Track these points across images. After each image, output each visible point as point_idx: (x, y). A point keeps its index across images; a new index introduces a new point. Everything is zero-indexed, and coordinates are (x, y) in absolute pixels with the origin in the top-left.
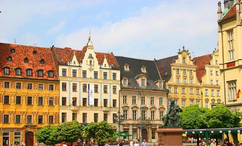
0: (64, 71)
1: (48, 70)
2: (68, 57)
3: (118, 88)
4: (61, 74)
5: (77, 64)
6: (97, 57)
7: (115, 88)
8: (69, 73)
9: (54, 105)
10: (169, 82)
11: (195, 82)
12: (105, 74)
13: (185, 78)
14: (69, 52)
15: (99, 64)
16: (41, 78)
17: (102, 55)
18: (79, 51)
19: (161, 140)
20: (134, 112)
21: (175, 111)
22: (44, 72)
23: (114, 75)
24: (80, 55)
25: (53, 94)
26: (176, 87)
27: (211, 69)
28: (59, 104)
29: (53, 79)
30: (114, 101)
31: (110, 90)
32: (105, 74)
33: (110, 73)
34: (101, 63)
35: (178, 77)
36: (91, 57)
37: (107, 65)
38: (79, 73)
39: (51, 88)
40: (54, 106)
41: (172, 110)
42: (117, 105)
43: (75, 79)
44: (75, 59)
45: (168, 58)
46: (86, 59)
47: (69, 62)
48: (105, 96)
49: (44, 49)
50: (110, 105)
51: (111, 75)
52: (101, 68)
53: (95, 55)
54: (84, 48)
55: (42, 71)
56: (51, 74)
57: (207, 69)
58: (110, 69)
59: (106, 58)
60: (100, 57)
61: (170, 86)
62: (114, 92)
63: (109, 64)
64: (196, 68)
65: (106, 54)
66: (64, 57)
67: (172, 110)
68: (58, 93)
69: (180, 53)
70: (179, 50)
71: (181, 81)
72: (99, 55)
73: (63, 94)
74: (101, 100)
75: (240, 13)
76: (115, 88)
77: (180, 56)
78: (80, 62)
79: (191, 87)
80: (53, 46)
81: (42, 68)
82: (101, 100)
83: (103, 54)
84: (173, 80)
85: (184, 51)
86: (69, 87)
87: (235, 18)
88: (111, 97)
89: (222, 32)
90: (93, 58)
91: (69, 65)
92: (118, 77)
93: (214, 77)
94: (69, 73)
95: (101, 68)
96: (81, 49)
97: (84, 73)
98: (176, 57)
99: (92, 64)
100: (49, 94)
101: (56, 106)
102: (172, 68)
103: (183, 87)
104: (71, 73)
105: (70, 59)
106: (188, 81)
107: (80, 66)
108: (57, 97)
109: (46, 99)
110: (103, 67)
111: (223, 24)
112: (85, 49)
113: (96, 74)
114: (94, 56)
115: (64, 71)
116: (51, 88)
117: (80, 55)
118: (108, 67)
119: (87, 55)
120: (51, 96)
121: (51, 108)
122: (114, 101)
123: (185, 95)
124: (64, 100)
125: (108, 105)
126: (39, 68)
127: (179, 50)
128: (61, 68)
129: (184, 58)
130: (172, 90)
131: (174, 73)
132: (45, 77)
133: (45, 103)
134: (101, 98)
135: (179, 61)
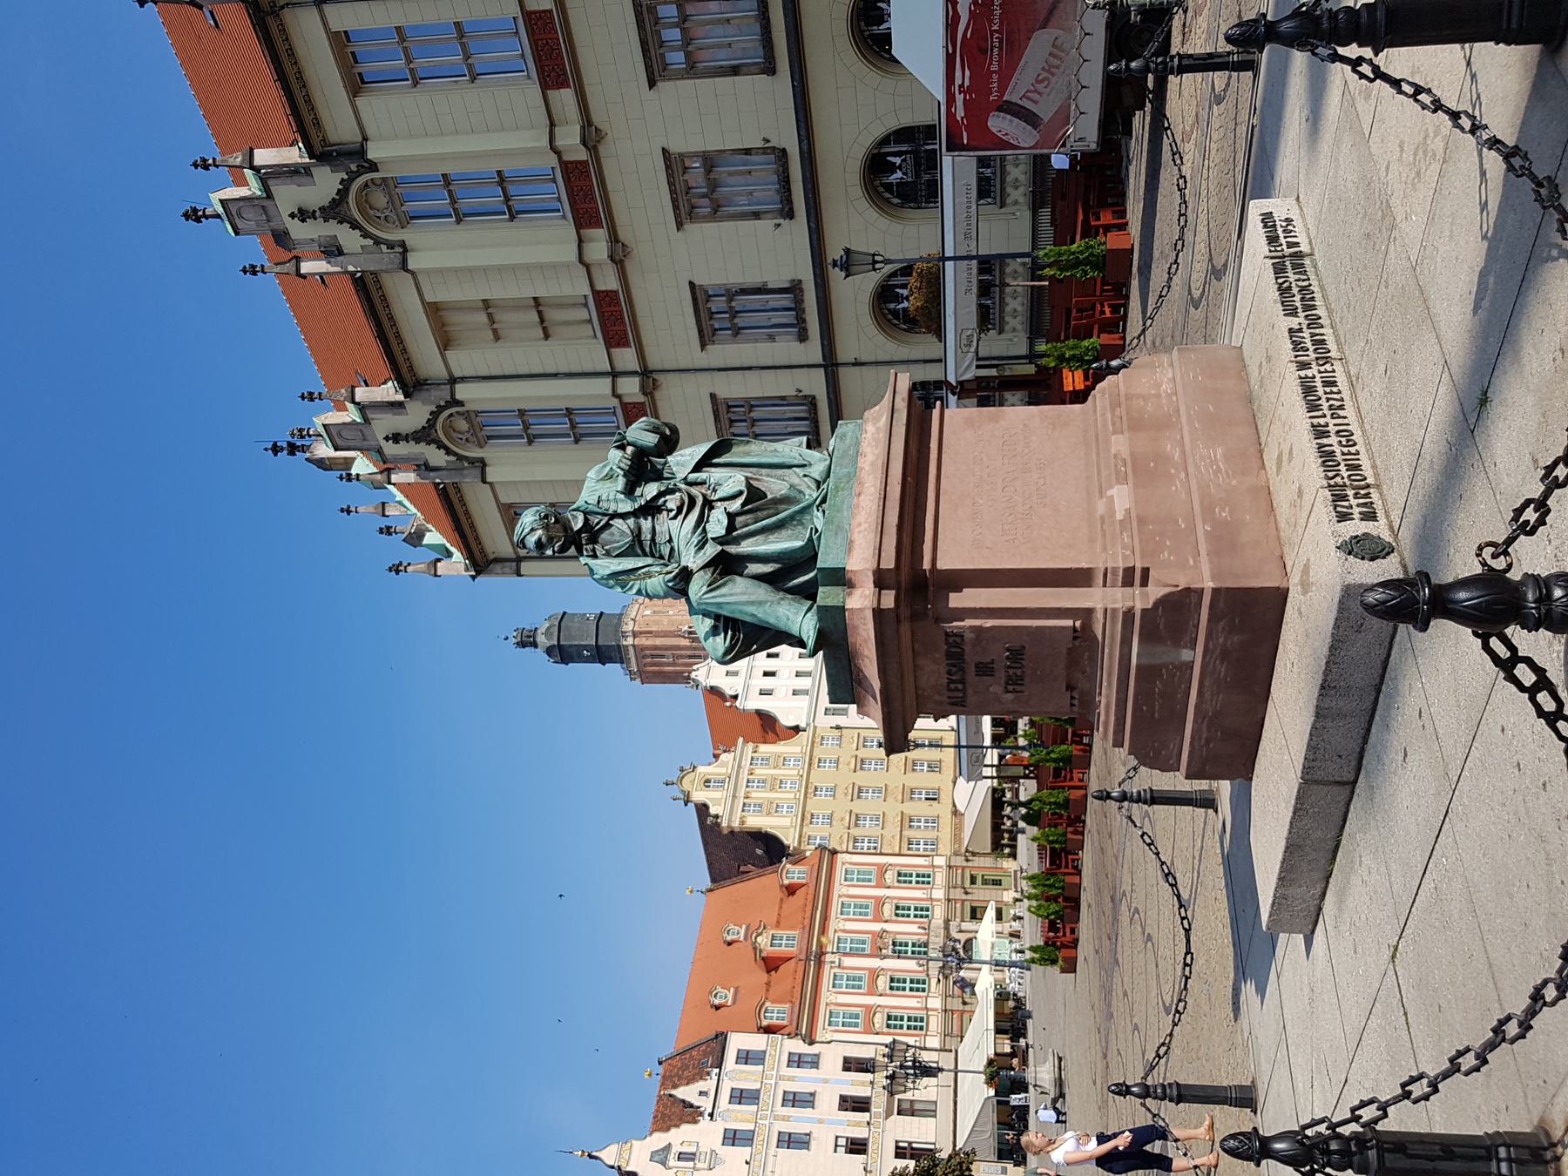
3: (798, 1046)
6: (668, 1129)
7: (797, 1061)
10: (790, 840)
11: (798, 749)
12: (740, 1097)
15: (695, 1122)
17: (665, 1107)
23: (746, 1057)
26: (806, 818)
30: (850, 1065)
31: (802, 1080)
32: (740, 1097)
33: (735, 1075)
34: (690, 1113)
37: (701, 1085)
41: (637, 534)
48: (828, 1102)
50: (862, 1084)
51: (742, 1072)
53: (656, 1135)
57: (753, 703)
59: (675, 1087)
62: (814, 1062)
63: (702, 1075)
64: (746, 742)
65: (663, 1085)
67: (637, 534)
74: (840, 1123)
77: (699, 796)
82: (840, 1123)
87: (451, 491)
90: (668, 1147)
92: (757, 1042)
99: (692, 1149)
103: (810, 790)
106: (790, 772)
110: (706, 1104)
111: (482, 551)
114: (658, 1140)
118: (709, 1084)
122: (850, 1065)
130: (819, 832)
131: (755, 822)
134: (832, 1122)
135: (717, 802)
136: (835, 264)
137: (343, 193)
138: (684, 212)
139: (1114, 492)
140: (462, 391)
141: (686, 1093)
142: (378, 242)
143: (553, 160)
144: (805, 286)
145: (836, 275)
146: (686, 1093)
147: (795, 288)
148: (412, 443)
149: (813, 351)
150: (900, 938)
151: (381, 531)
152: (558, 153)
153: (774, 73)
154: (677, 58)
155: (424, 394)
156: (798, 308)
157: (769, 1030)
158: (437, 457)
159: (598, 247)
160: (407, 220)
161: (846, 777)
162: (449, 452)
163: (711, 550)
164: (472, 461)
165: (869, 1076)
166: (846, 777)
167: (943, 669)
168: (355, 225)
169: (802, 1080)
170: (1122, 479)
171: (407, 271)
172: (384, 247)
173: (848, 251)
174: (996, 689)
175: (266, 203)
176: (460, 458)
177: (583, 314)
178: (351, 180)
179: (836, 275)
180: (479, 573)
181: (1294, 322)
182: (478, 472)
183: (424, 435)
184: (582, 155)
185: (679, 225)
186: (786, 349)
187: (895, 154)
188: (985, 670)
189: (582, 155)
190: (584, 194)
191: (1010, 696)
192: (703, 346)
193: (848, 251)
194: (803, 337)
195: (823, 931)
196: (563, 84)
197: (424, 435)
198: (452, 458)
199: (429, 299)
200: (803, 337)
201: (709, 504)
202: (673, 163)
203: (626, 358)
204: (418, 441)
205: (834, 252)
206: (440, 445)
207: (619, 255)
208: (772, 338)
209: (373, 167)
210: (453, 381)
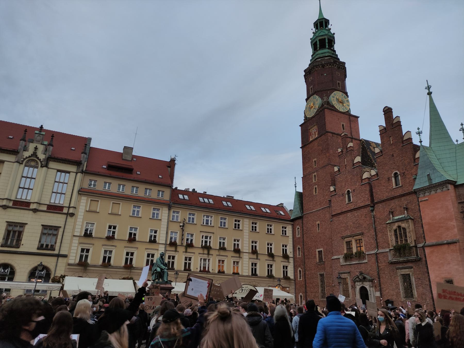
137: (38, 158)
138: (10, 224)
142: (24, 159)
154: (46, 231)
159: (11, 204)
168: (29, 157)
175: (40, 142)
178: (40, 161)
187: (8, 271)
196: (48, 208)
199: (5, 162)
202: (23, 225)
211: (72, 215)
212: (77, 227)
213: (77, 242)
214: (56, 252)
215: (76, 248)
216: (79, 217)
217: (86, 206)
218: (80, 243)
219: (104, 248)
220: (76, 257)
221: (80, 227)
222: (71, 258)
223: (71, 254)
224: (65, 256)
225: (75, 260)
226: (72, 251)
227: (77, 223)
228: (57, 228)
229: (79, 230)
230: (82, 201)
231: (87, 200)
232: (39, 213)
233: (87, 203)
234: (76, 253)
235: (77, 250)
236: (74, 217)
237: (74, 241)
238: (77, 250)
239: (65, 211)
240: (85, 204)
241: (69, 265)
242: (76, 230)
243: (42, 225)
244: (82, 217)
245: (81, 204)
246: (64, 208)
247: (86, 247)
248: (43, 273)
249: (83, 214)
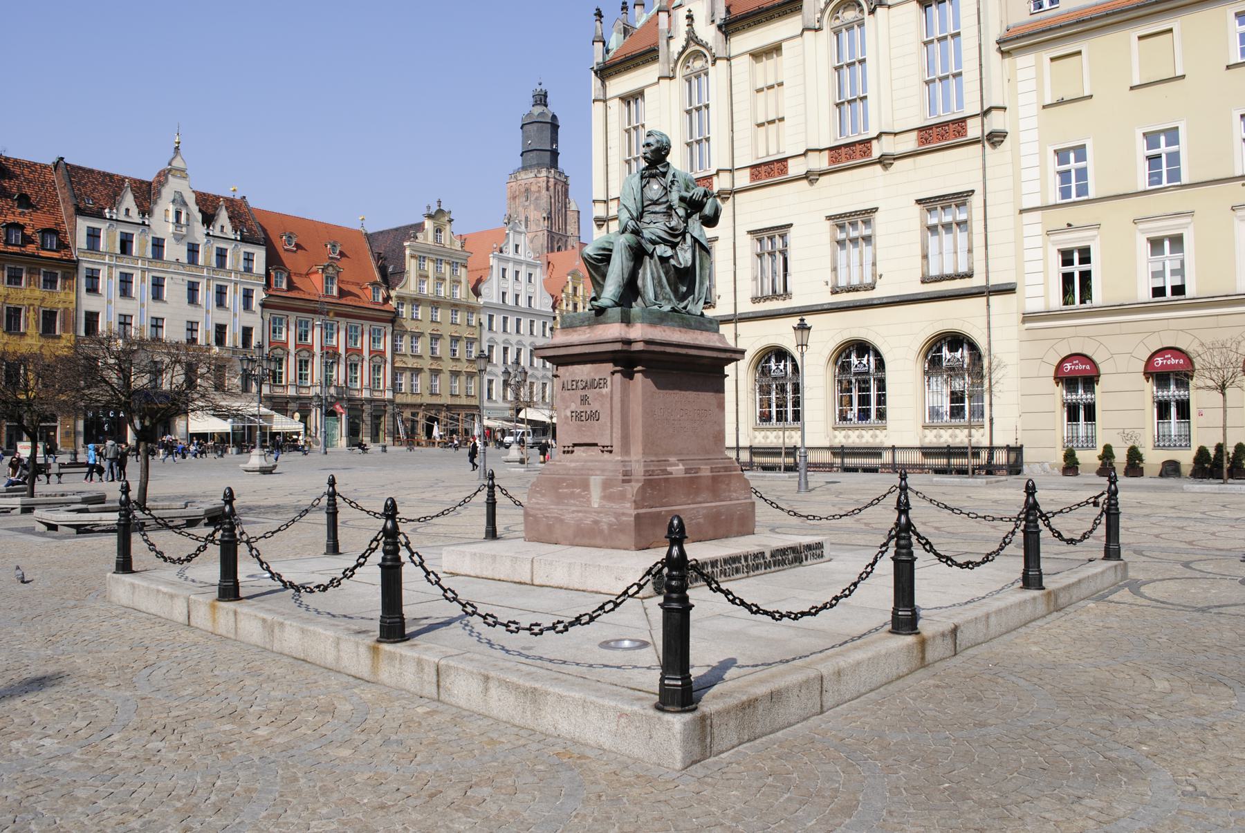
0: (93, 235)
1: (38, 227)
2: (107, 194)
3: (259, 295)
4: (81, 241)
5: (137, 218)
7: (248, 295)
8: (109, 240)
9: (58, 333)
12: (221, 254)
13: (440, 280)
14: (112, 185)
16: (16, 249)
17: (212, 201)
18: (142, 182)
19: (594, 416)
20: (303, 364)
21: (681, 212)
22: (29, 231)
23: (249, 258)
24: (146, 194)
25: (59, 298)
26: (416, 302)
27: (503, 265)
28: (75, 331)
29: (56, 255)
30: (247, 332)
31: (233, 298)
32: (221, 254)
34: (208, 220)
35: (423, 277)
36: (179, 201)
38: (142, 246)
39: (50, 282)
40: (59, 337)
42: (255, 340)
43: (126, 261)
44: (129, 201)
45: (397, 229)
46: (164, 207)
47: (111, 209)
48: (221, 317)
49: (32, 166)
50: (235, 340)
52: (208, 234)
53: (193, 196)
54: (159, 175)
55: (21, 227)
56: (52, 241)
58: (236, 240)
60: (208, 208)
61: (402, 300)
62: (247, 306)
63: (235, 229)
65: (226, 200)
66: (96, 195)
68: (73, 297)
69: (430, 216)
70: (429, 207)
71: (428, 289)
72: (206, 200)
73: (89, 303)
75: (671, 37)
76: (248, 295)
77: (429, 224)
78: (145, 211)
79: (455, 307)
80: (62, 159)
81: (21, 220)
83: (218, 198)
84: (410, 285)
85: (440, 211)
86: (108, 283)
88: (236, 319)
89: (605, 101)
90: (185, 204)
91: (108, 216)
92: (259, 265)
93: (510, 285)
94: (109, 240)
95: (208, 234)
96: (150, 177)
97: (158, 244)
98: (419, 227)
100: (43, 299)
101: (64, 335)
102: (408, 252)
103: (436, 304)
104: (114, 242)
105: (114, 199)
107: (143, 224)
108: (66, 309)
109: (32, 313)
112: (163, 176)
113: (193, 250)
114: (191, 199)
115: (93, 235)
116: (50, 282)
117: (146, 194)
119: (167, 193)
120: (48, 305)
121: (51, 342)
122: (247, 332)
123: (439, 327)
124: (92, 318)
125: (229, 342)
126: (10, 219)
127: (429, 207)
128: (83, 224)
129: (438, 231)
130: (405, 311)
131: (411, 265)
132: (31, 249)
133: (27, 326)
135: (426, 238)
136: (802, 320)
138: (840, 220)
139: (681, 467)
140: (721, 64)
141: (223, 218)
143: (873, 133)
144: (788, 301)
145: (795, 321)
146: (223, 218)
147: (786, 294)
148: (687, 28)
149: (746, 307)
150: (335, 367)
151: (624, 3)
152: (878, 137)
153: (923, 282)
155: (721, 36)
156: (775, 296)
157: (268, 275)
158: (677, 45)
160: (837, 32)
161: (447, 330)
162: (681, 54)
163: (650, 247)
164: (673, 70)
165: (240, 346)
166: (447, 330)
167: (584, 378)
169: (233, 298)
170: (687, 471)
171: (803, 30)
172: (819, 15)
173: (809, 329)
174: (573, 407)
176: (676, 62)
177: (773, 151)
179: (795, 321)
180: (596, 73)
181: (768, 555)
182: (666, 74)
183: (692, 38)
184: (876, 154)
185: (829, 218)
186: (747, 289)
188: (584, 400)
189: (877, 150)
190: (850, 154)
191: (569, 414)
192: (750, 232)
193: (809, 329)
194: (755, 300)
195: (338, 314)
196: (923, 140)
197: (692, 38)
198: (676, 56)
200: (755, 300)
201: (674, 246)
203: (743, 179)
204: (688, 33)
205: (809, 320)
206: (685, 49)
207: (810, 177)
208: (755, 279)
209: (872, 12)
210: (729, 59)
211: (995, 138)
212: (1025, 175)
213: (1038, 229)
214: (978, 281)
215: (1039, 254)
216: (1024, 137)
217: (1039, 90)
218: (1049, 233)
219: (1143, 231)
220: (1045, 284)
221: (1036, 173)
222: (1029, 291)
223: (1029, 279)
224: (1009, 290)
225: (1046, 296)
226: (1028, 267)
227: (1025, 162)
228: (960, 198)
229: (1036, 186)
230: (1021, 75)
231: (1038, 66)
232: (897, 164)
233: (1039, 78)
234: (1045, 272)
235: (1045, 259)
236: (1007, 140)
237: (1027, 231)
238: (1045, 259)
239: (974, 130)
240: (1032, 85)
241: (1027, 318)
242: (1026, 188)
243: (919, 202)
244: (1034, 135)
245: (1021, 87)
246: (969, 122)
247: (1073, 240)
248: (958, 355)
249: (1034, 122)
